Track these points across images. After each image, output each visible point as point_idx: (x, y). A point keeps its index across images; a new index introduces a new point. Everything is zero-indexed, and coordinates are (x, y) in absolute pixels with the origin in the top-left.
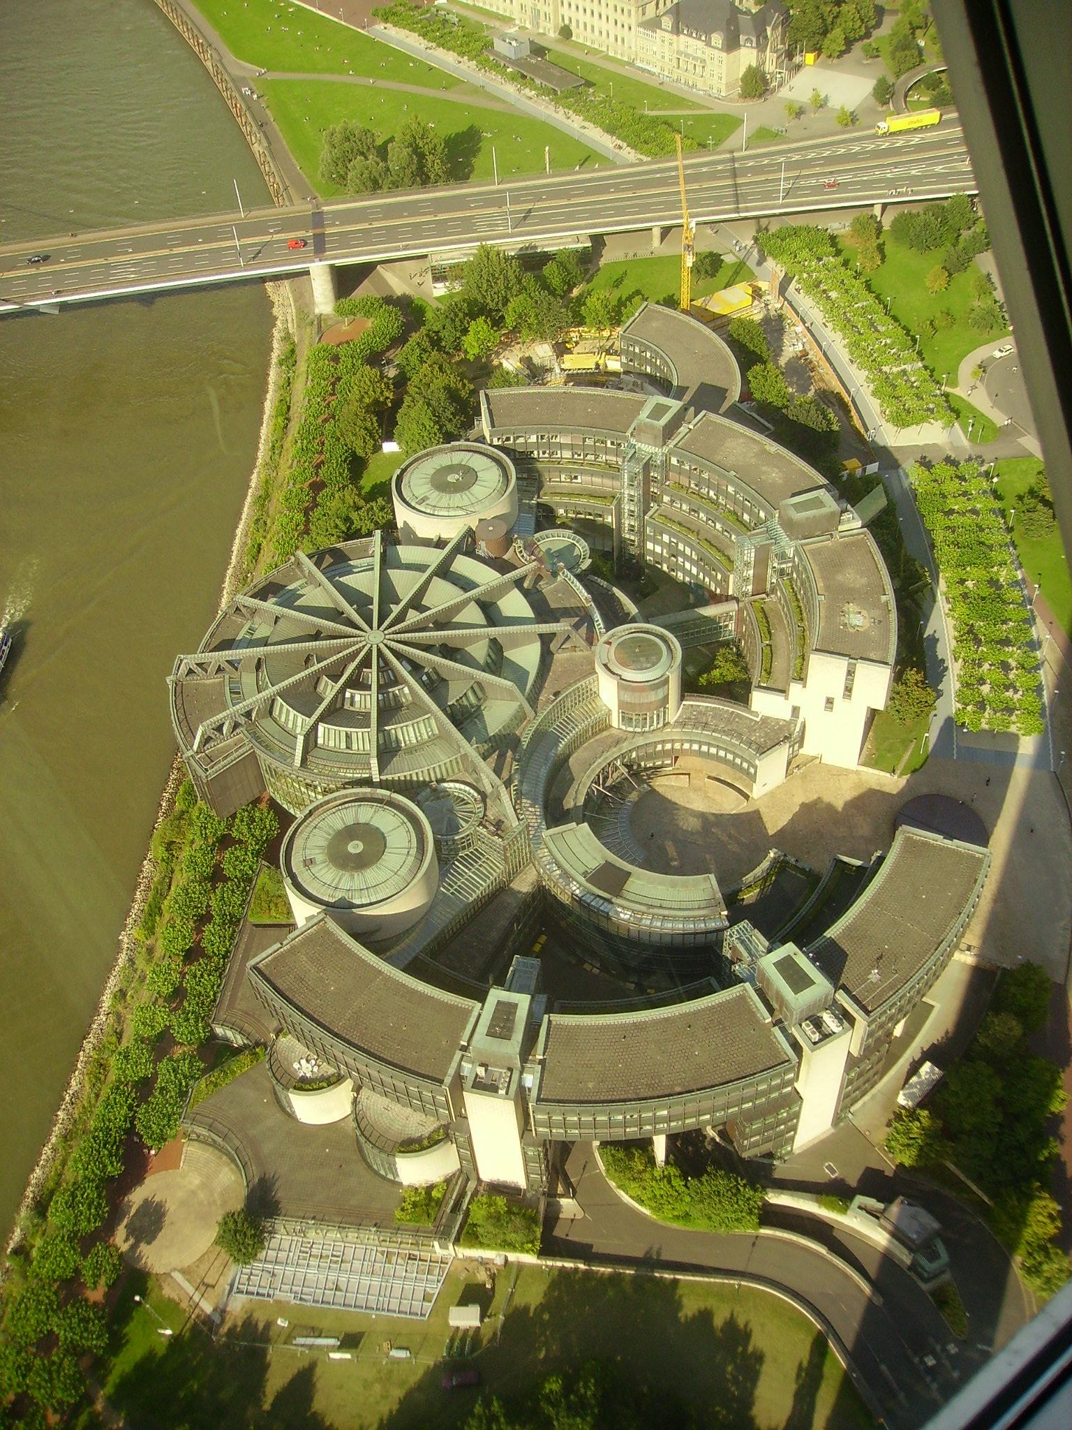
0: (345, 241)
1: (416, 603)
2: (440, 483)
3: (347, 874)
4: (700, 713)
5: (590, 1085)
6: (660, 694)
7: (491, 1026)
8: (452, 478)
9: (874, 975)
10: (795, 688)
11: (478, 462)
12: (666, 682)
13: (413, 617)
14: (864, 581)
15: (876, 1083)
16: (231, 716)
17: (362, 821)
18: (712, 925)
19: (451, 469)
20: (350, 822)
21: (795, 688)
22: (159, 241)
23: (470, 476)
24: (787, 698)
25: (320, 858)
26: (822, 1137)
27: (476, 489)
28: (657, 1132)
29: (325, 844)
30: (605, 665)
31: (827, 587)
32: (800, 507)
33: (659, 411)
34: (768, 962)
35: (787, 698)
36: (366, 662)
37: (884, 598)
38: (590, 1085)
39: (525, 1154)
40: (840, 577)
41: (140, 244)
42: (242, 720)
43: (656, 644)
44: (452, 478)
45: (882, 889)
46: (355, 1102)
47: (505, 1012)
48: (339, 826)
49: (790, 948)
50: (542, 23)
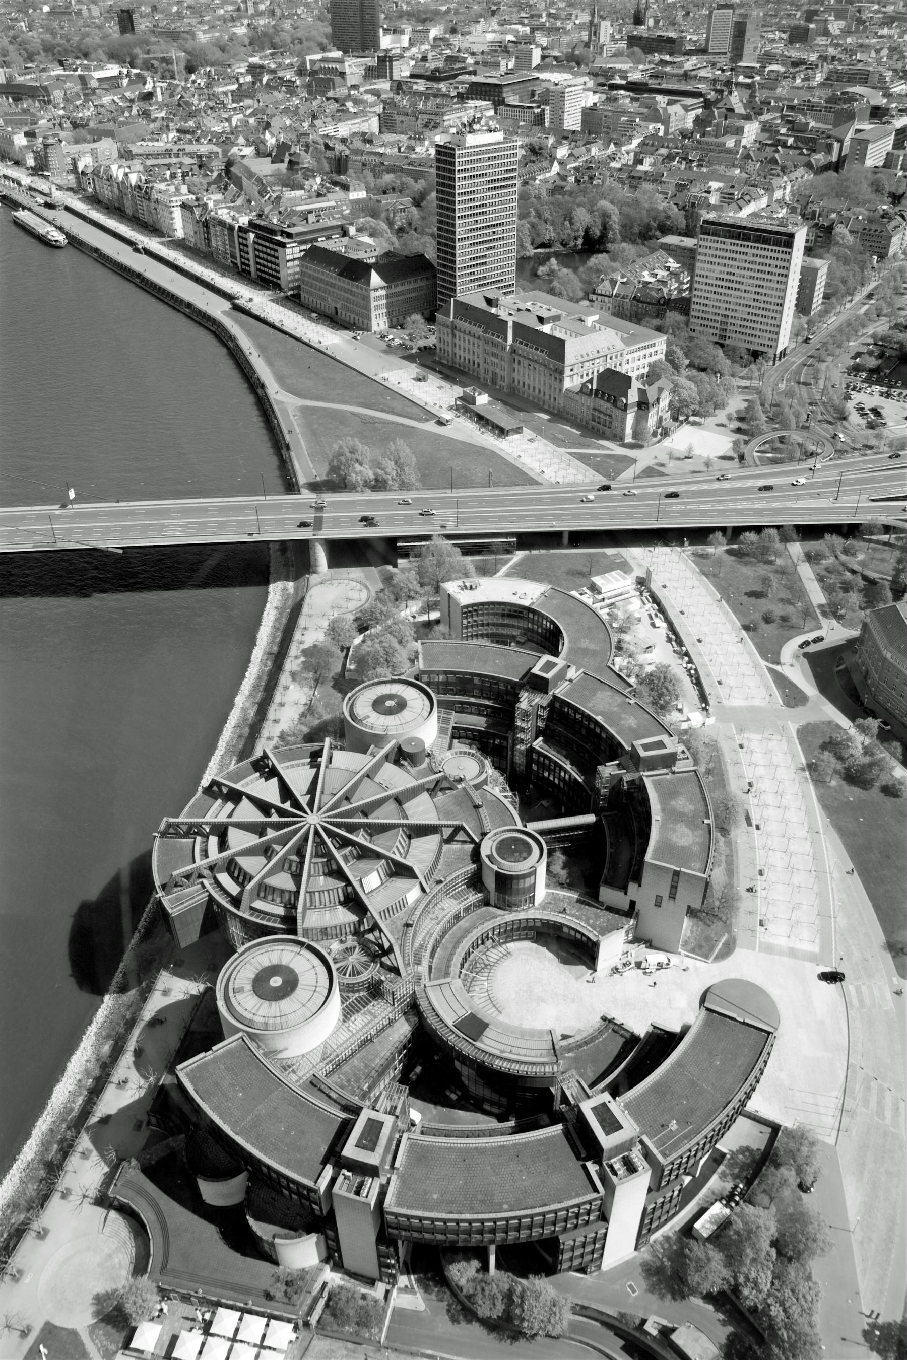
0: (337, 523)
1: (347, 798)
2: (378, 704)
3: (267, 1003)
4: (559, 899)
5: (435, 1196)
6: (528, 882)
7: (360, 1140)
8: (389, 703)
9: (674, 1126)
10: (632, 887)
11: (410, 694)
12: (534, 873)
13: (346, 807)
14: (692, 807)
15: (674, 1215)
16: (199, 868)
17: (284, 963)
18: (548, 1069)
19: (390, 697)
20: (275, 961)
21: (632, 887)
22: (204, 511)
23: (401, 705)
24: (626, 893)
25: (248, 987)
26: (627, 1258)
27: (405, 713)
28: (492, 1241)
29: (253, 976)
30: (488, 857)
31: (663, 810)
32: (646, 747)
33: (549, 666)
34: (587, 1106)
35: (626, 893)
36: (306, 839)
37: (706, 821)
38: (435, 1196)
39: (378, 1249)
40: (673, 803)
41: (186, 512)
42: (206, 872)
43: (528, 844)
44: (389, 703)
45: (686, 1053)
46: (248, 1190)
47: (374, 1127)
48: (266, 963)
49: (606, 1097)
50: (499, 382)
